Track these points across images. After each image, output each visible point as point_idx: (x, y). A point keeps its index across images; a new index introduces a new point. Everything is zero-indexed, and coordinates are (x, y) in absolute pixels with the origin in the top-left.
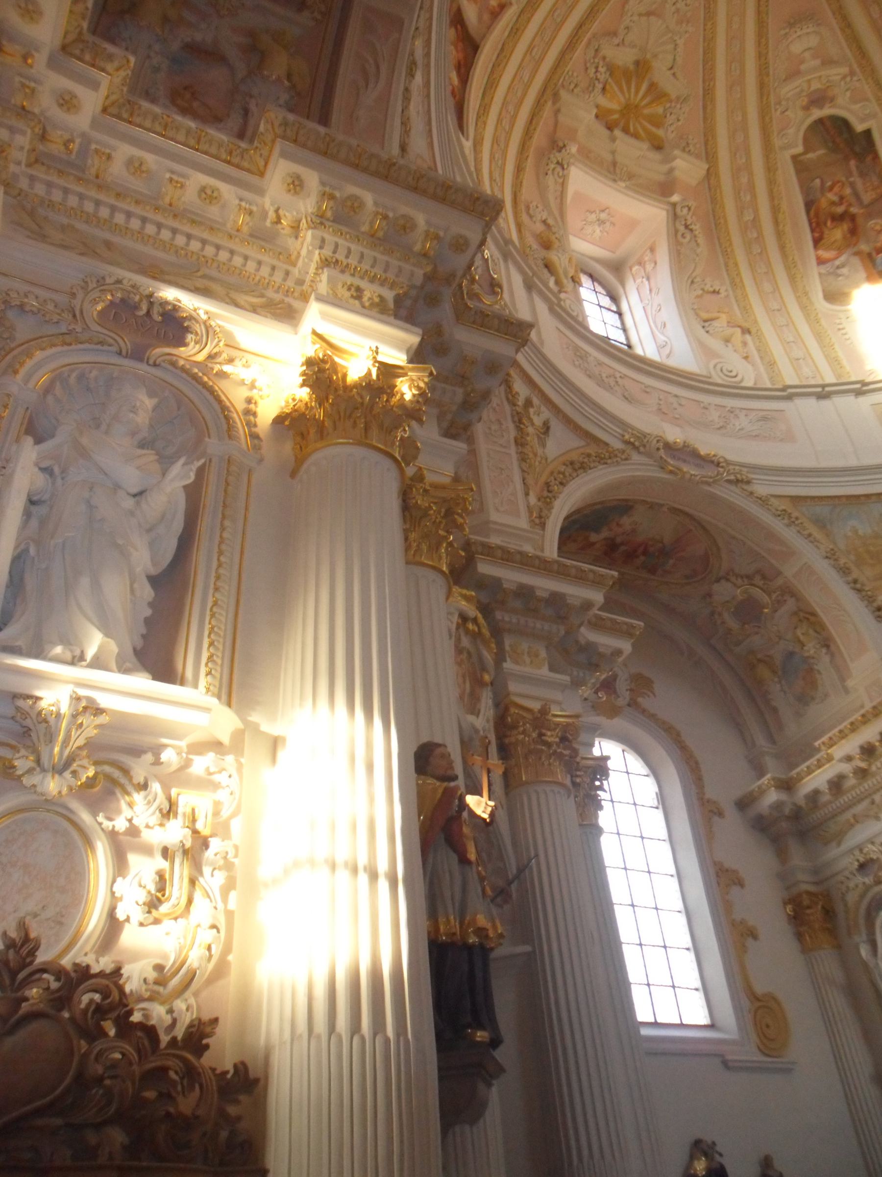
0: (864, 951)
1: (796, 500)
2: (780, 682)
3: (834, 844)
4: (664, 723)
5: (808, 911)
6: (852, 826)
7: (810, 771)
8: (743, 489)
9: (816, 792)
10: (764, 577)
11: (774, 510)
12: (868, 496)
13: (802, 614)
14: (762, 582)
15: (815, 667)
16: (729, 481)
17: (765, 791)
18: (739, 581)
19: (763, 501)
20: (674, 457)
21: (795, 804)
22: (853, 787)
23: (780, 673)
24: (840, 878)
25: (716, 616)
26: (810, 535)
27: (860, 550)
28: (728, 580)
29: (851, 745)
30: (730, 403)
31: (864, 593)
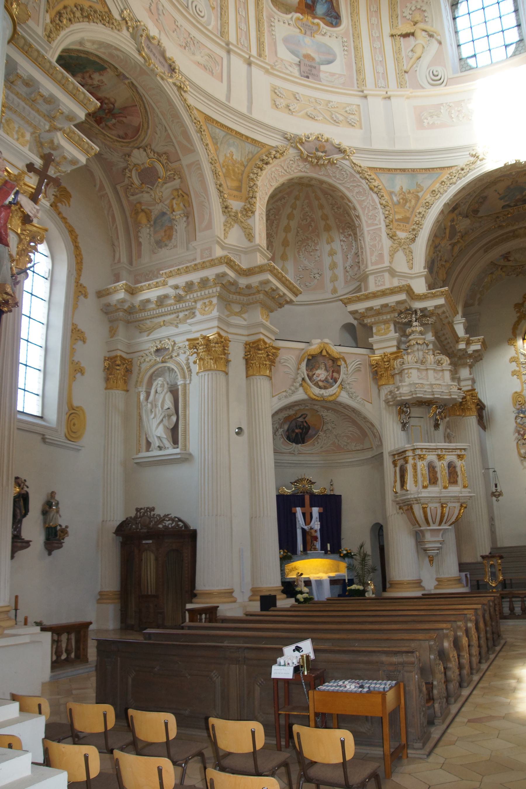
0: (142, 397)
1: (209, 119)
2: (149, 228)
3: (146, 333)
4: (70, 226)
5: (118, 368)
6: (161, 326)
7: (149, 287)
8: (181, 95)
9: (148, 301)
10: (168, 159)
11: (193, 118)
12: (247, 138)
13: (180, 192)
14: (166, 161)
15: (175, 227)
16: (174, 84)
17: (118, 290)
18: (151, 155)
19: (189, 108)
20: (149, 48)
21: (132, 304)
22: (171, 305)
23: (152, 223)
24: (141, 353)
25: (127, 171)
26: (207, 145)
27: (230, 168)
28: (145, 150)
29: (181, 280)
30: (194, 33)
31: (222, 194)
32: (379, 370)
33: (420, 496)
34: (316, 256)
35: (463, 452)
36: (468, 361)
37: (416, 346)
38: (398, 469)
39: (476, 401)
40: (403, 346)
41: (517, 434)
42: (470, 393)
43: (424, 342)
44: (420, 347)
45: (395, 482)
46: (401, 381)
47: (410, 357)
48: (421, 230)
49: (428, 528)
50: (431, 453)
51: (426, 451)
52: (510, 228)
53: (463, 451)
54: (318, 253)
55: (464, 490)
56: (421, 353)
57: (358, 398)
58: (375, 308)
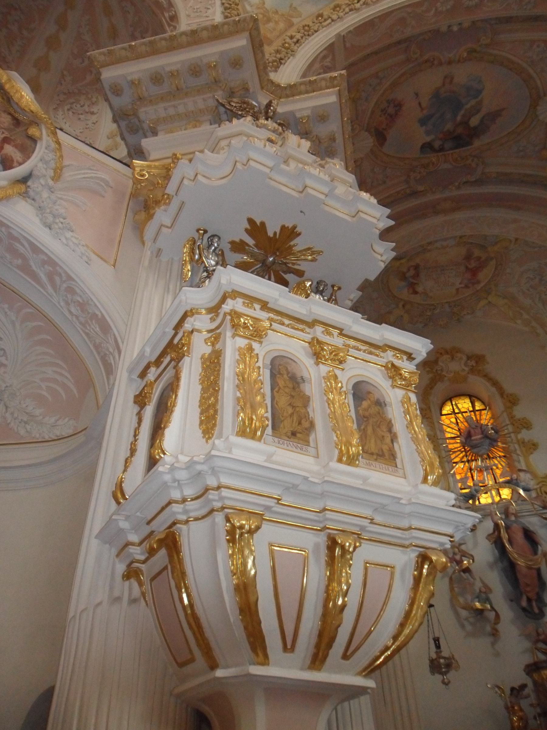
34: (90, 123)
48: (291, 57)
49: (257, 670)
52: (430, 198)
54: (94, 118)
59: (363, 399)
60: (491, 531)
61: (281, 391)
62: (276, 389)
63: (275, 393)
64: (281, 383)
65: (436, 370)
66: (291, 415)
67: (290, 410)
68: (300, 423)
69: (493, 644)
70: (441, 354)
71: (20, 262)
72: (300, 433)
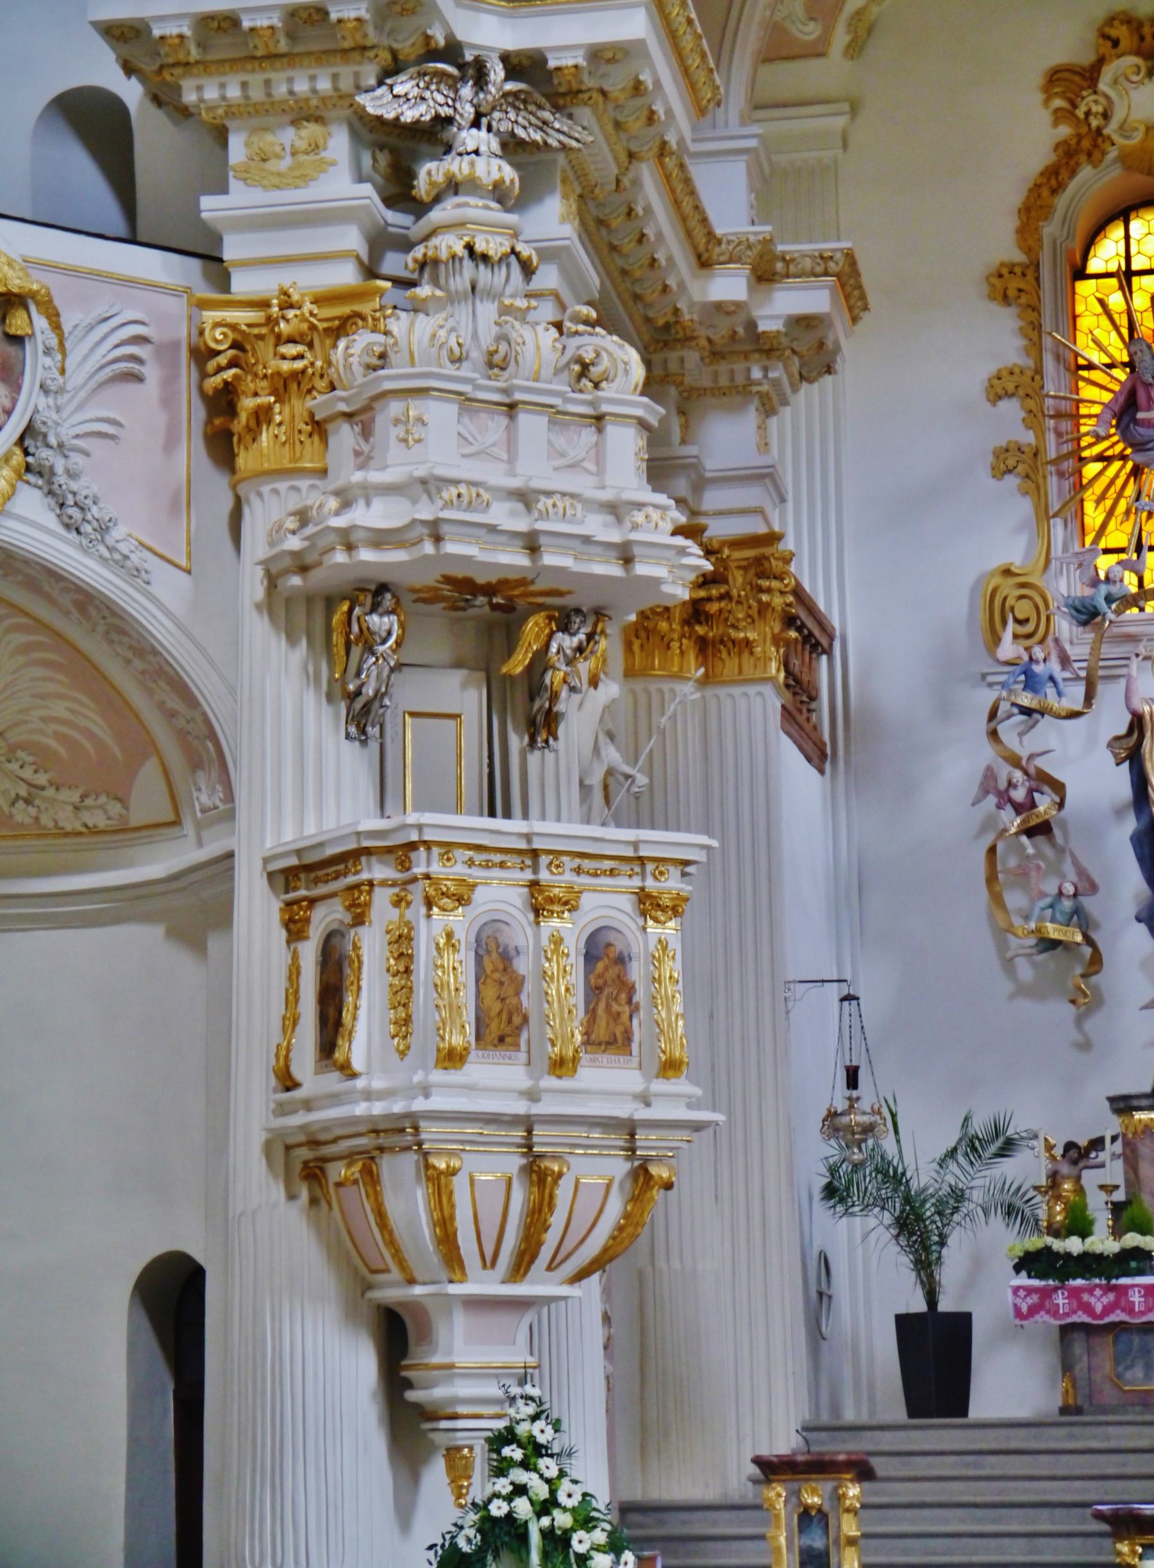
32: (250, 384)
33: (419, 1105)
35: (672, 884)
36: (757, 374)
37: (468, 264)
38: (309, 952)
39: (778, 601)
40: (394, 263)
41: (992, 800)
42: (750, 553)
43: (513, 251)
44: (484, 273)
45: (291, 1022)
46: (363, 460)
47: (424, 325)
50: (496, 873)
51: (471, 863)
53: (675, 872)
55: (659, 1086)
56: (487, 311)
57: (118, 533)
58: (246, 24)
59: (599, 959)
60: (1122, 730)
61: (489, 981)
62: (482, 980)
63: (481, 986)
64: (489, 967)
65: (1088, 114)
66: (500, 1013)
67: (497, 1007)
68: (510, 1021)
69: (1079, 1021)
70: (1116, 43)
71: (20, 578)
72: (509, 1036)
